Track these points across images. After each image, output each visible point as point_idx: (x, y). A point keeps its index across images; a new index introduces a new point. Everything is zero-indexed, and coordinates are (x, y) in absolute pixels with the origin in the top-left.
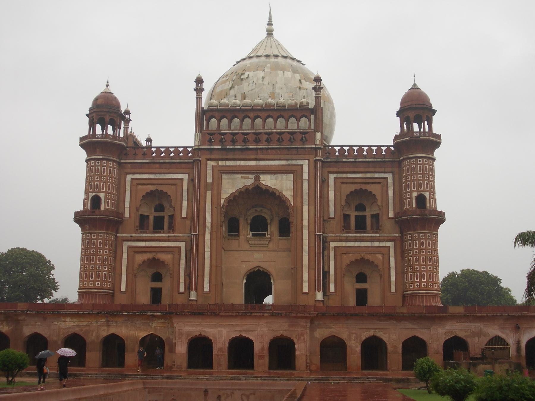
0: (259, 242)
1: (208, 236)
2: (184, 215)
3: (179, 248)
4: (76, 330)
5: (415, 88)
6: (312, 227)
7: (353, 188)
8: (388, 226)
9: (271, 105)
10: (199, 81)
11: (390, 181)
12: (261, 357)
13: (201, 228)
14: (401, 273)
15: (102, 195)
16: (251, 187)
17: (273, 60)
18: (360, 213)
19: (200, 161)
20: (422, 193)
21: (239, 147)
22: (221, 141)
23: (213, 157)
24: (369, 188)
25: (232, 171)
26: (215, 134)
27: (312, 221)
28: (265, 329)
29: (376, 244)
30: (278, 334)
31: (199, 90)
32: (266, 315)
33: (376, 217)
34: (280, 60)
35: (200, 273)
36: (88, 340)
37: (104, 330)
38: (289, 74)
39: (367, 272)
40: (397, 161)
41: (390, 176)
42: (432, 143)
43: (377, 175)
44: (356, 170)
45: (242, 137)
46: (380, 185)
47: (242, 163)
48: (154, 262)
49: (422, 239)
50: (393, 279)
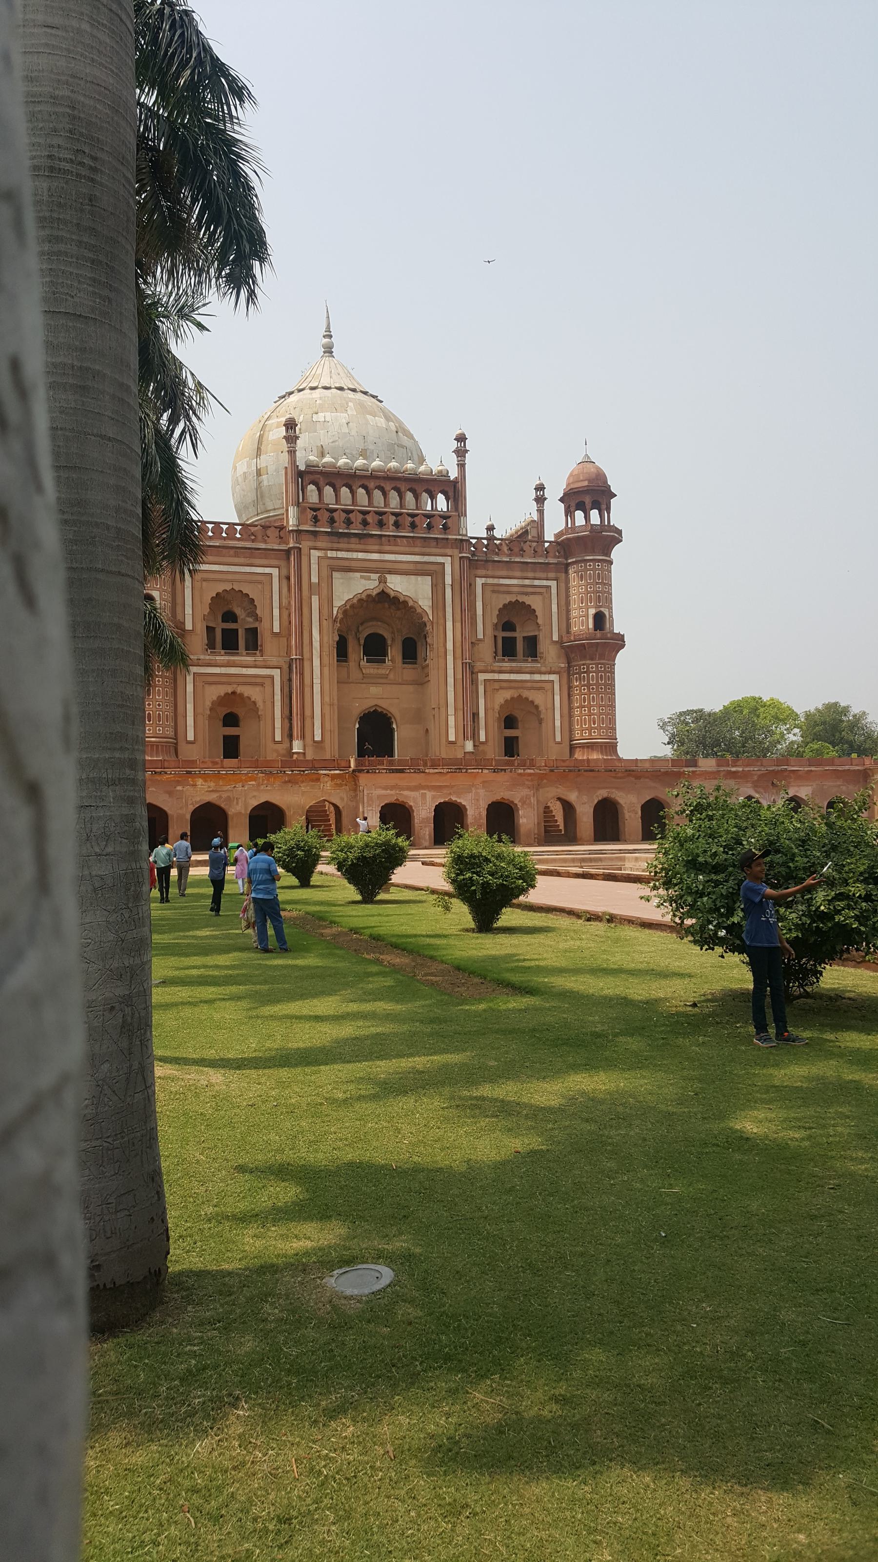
0: (376, 671)
1: (316, 662)
2: (276, 629)
3: (272, 677)
4: (212, 798)
5: (588, 461)
6: (459, 651)
8: (549, 651)
11: (554, 591)
13: (306, 649)
16: (375, 593)
17: (351, 395)
19: (300, 549)
20: (602, 609)
21: (356, 531)
22: (332, 521)
23: (319, 544)
25: (347, 568)
26: (319, 509)
27: (458, 644)
28: (482, 792)
29: (537, 677)
30: (497, 797)
31: (291, 439)
32: (485, 771)
34: (360, 396)
35: (308, 713)
36: (231, 811)
37: (254, 796)
39: (518, 714)
40: (563, 564)
41: (553, 584)
44: (511, 573)
45: (360, 517)
46: (540, 597)
47: (361, 555)
48: (232, 697)
49: (601, 672)
50: (558, 723)
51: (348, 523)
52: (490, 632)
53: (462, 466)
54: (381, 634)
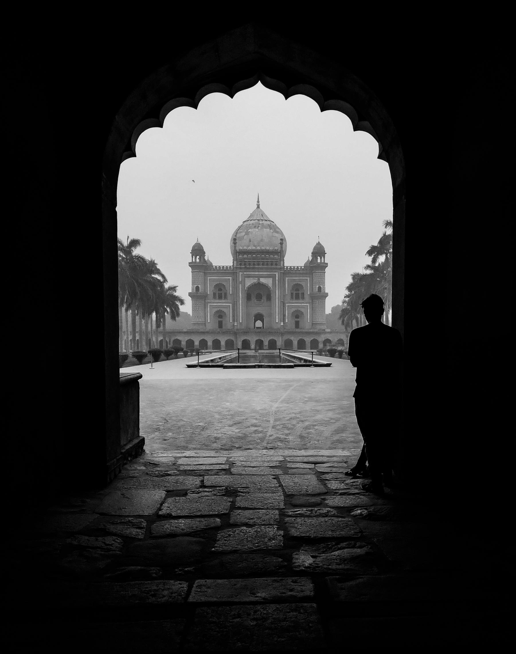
1: (241, 302)
3: (229, 306)
5: (319, 244)
7: (295, 283)
9: (263, 250)
10: (235, 240)
11: (309, 280)
12: (265, 346)
15: (200, 286)
18: (297, 292)
22: (245, 264)
25: (249, 276)
29: (303, 304)
31: (235, 243)
33: (303, 294)
34: (264, 222)
41: (308, 278)
42: (325, 265)
45: (253, 263)
47: (253, 273)
50: (309, 317)
51: (250, 264)
52: (289, 291)
53: (282, 247)
54: (259, 293)
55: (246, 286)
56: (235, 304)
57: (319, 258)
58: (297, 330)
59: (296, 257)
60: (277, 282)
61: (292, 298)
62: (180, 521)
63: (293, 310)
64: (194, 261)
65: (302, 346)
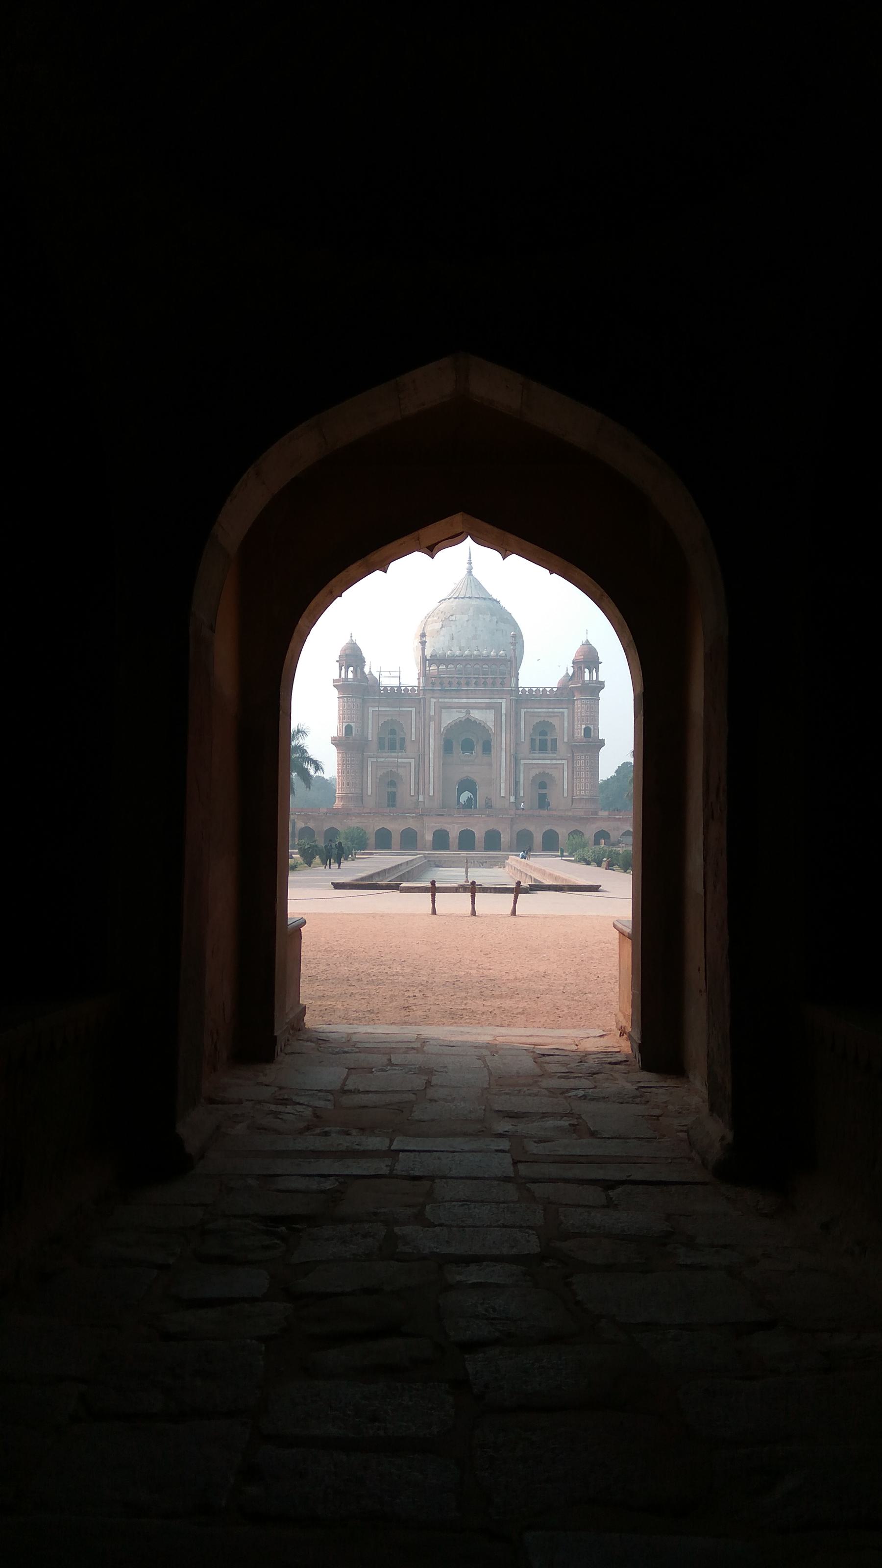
1: (432, 756)
2: (413, 739)
5: (587, 643)
8: (562, 748)
10: (423, 635)
11: (566, 714)
14: (571, 782)
15: (353, 725)
17: (474, 602)
22: (441, 684)
23: (435, 696)
24: (550, 720)
29: (554, 762)
31: (423, 643)
35: (426, 781)
38: (488, 618)
41: (566, 711)
43: (556, 710)
47: (457, 700)
50: (565, 787)
55: (443, 725)
56: (421, 759)
57: (586, 670)
58: (544, 812)
59: (542, 668)
60: (504, 717)
61: (533, 749)
62: (370, 1095)
63: (534, 772)
64: (343, 676)
65: (550, 844)
